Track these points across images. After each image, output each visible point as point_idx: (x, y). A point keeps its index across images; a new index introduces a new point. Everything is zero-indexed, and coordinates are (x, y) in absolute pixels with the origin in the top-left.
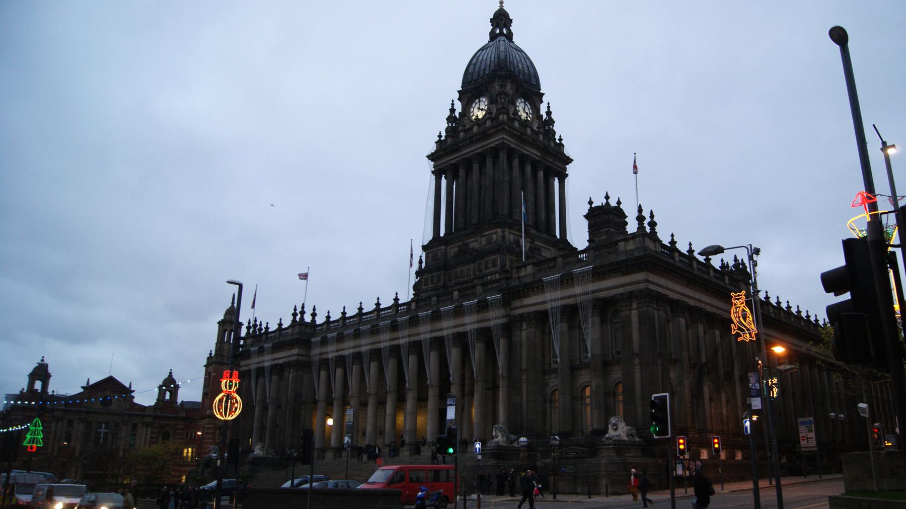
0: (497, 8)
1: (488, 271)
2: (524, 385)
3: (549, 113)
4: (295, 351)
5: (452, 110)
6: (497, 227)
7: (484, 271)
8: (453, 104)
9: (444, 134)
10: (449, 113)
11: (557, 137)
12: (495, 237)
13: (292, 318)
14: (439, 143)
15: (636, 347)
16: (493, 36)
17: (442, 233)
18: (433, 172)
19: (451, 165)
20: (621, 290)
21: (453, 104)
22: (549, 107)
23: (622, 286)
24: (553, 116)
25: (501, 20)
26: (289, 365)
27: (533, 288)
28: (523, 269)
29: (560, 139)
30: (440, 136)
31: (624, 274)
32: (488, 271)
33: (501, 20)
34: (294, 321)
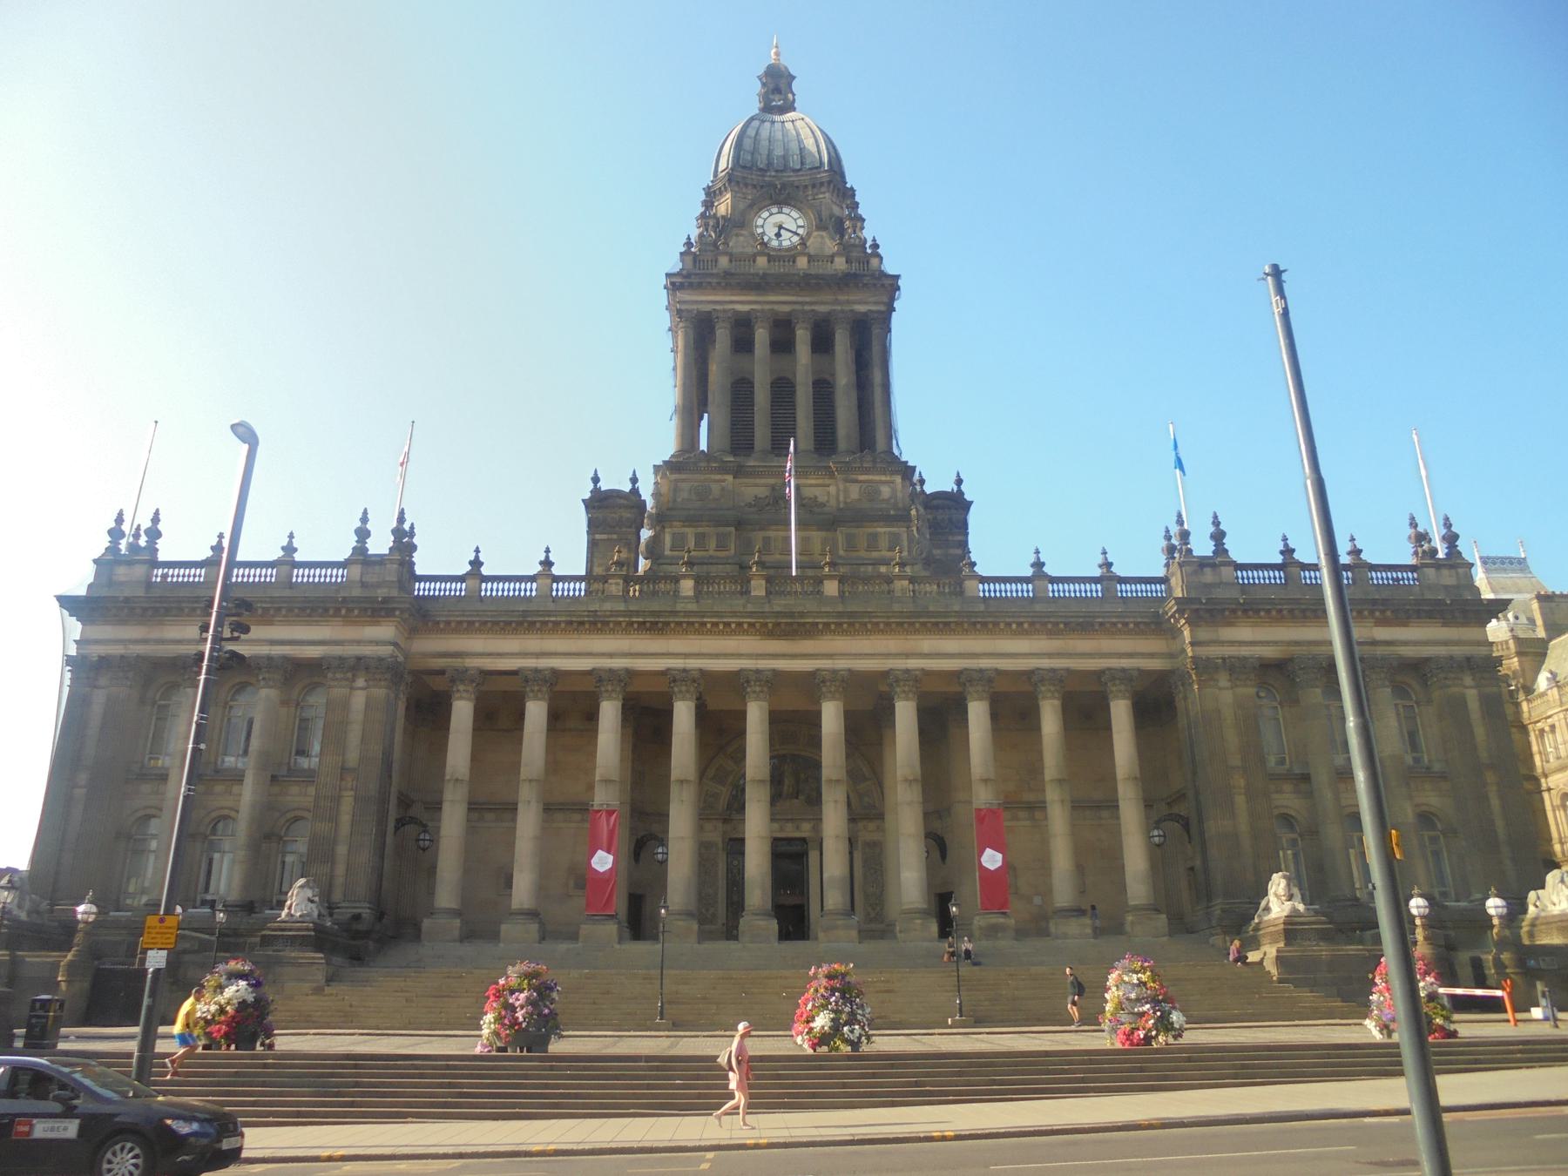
1: (875, 554)
2: (1240, 800)
4: (385, 631)
6: (893, 473)
7: (863, 554)
12: (886, 491)
13: (352, 541)
15: (1483, 755)
17: (703, 446)
19: (736, 312)
20: (1442, 651)
23: (1446, 643)
26: (358, 665)
27: (1257, 611)
28: (1208, 570)
31: (1445, 625)
32: (875, 554)
34: (360, 550)
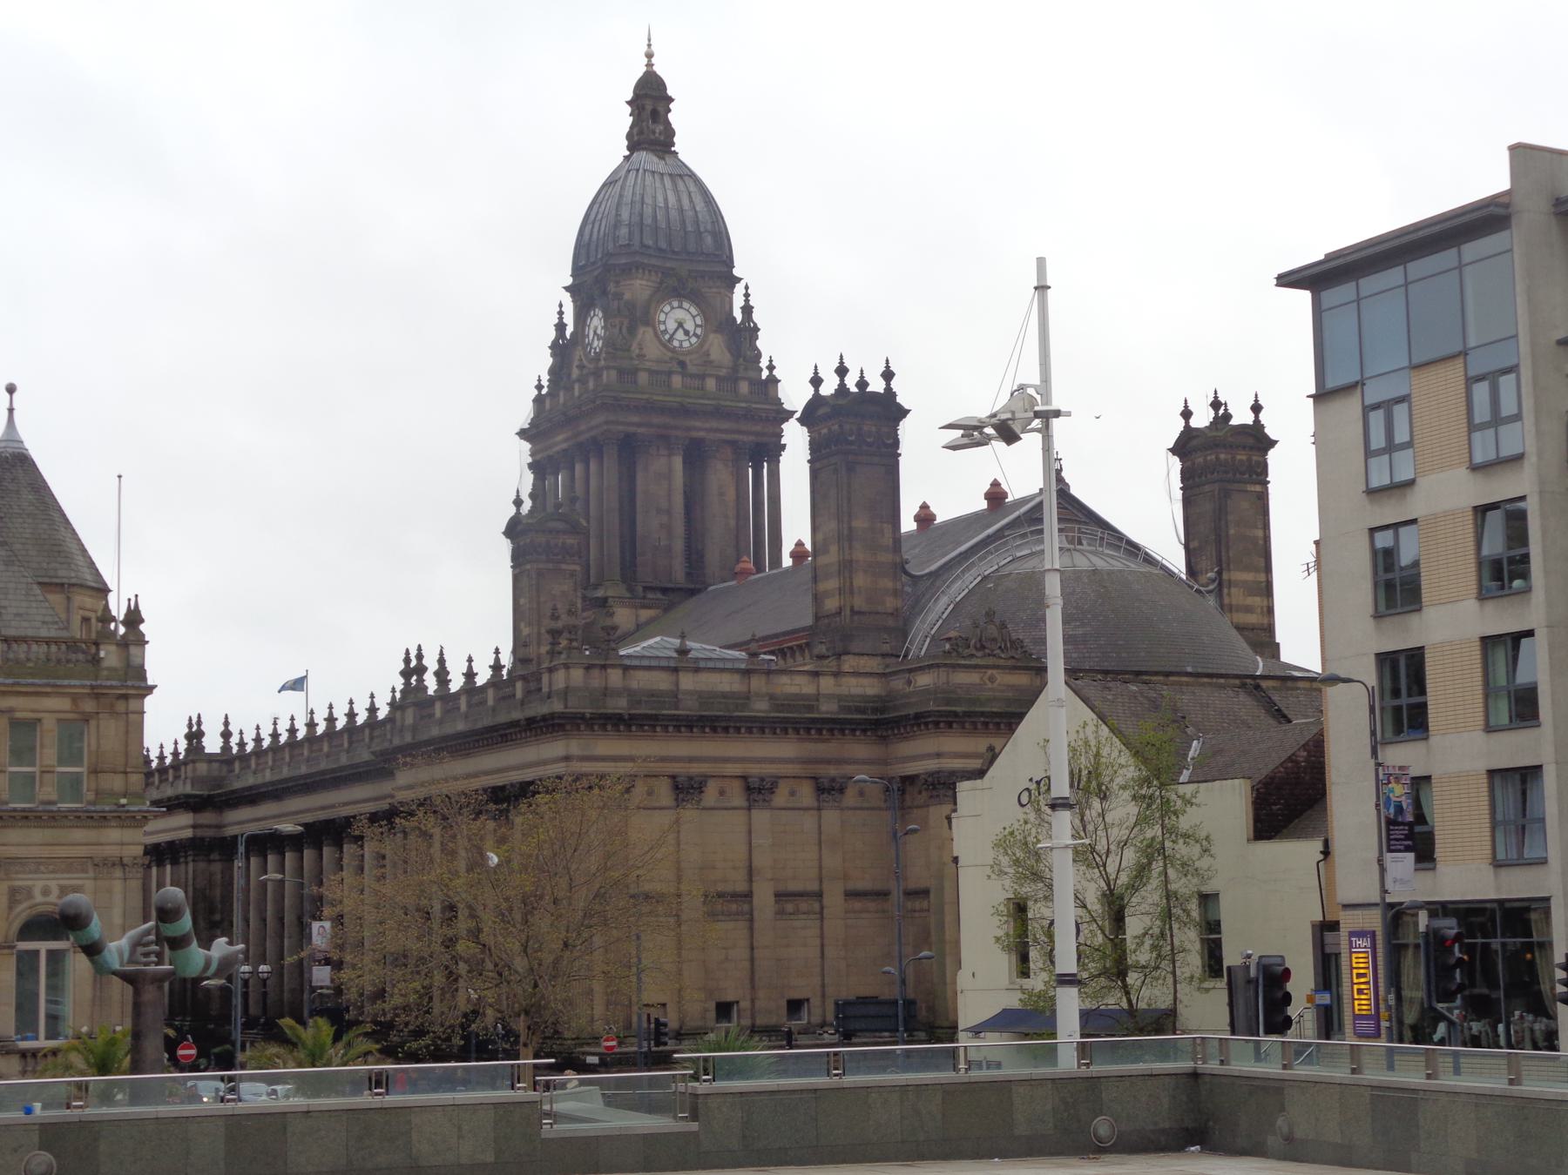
0: (640, 71)
3: (747, 310)
5: (560, 327)
8: (561, 313)
9: (545, 383)
10: (552, 335)
11: (764, 363)
14: (539, 401)
16: (634, 145)
18: (530, 466)
21: (561, 313)
22: (747, 295)
24: (755, 317)
25: (650, 101)
29: (771, 368)
30: (539, 387)
33: (650, 101)
